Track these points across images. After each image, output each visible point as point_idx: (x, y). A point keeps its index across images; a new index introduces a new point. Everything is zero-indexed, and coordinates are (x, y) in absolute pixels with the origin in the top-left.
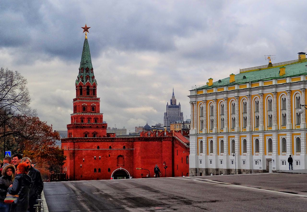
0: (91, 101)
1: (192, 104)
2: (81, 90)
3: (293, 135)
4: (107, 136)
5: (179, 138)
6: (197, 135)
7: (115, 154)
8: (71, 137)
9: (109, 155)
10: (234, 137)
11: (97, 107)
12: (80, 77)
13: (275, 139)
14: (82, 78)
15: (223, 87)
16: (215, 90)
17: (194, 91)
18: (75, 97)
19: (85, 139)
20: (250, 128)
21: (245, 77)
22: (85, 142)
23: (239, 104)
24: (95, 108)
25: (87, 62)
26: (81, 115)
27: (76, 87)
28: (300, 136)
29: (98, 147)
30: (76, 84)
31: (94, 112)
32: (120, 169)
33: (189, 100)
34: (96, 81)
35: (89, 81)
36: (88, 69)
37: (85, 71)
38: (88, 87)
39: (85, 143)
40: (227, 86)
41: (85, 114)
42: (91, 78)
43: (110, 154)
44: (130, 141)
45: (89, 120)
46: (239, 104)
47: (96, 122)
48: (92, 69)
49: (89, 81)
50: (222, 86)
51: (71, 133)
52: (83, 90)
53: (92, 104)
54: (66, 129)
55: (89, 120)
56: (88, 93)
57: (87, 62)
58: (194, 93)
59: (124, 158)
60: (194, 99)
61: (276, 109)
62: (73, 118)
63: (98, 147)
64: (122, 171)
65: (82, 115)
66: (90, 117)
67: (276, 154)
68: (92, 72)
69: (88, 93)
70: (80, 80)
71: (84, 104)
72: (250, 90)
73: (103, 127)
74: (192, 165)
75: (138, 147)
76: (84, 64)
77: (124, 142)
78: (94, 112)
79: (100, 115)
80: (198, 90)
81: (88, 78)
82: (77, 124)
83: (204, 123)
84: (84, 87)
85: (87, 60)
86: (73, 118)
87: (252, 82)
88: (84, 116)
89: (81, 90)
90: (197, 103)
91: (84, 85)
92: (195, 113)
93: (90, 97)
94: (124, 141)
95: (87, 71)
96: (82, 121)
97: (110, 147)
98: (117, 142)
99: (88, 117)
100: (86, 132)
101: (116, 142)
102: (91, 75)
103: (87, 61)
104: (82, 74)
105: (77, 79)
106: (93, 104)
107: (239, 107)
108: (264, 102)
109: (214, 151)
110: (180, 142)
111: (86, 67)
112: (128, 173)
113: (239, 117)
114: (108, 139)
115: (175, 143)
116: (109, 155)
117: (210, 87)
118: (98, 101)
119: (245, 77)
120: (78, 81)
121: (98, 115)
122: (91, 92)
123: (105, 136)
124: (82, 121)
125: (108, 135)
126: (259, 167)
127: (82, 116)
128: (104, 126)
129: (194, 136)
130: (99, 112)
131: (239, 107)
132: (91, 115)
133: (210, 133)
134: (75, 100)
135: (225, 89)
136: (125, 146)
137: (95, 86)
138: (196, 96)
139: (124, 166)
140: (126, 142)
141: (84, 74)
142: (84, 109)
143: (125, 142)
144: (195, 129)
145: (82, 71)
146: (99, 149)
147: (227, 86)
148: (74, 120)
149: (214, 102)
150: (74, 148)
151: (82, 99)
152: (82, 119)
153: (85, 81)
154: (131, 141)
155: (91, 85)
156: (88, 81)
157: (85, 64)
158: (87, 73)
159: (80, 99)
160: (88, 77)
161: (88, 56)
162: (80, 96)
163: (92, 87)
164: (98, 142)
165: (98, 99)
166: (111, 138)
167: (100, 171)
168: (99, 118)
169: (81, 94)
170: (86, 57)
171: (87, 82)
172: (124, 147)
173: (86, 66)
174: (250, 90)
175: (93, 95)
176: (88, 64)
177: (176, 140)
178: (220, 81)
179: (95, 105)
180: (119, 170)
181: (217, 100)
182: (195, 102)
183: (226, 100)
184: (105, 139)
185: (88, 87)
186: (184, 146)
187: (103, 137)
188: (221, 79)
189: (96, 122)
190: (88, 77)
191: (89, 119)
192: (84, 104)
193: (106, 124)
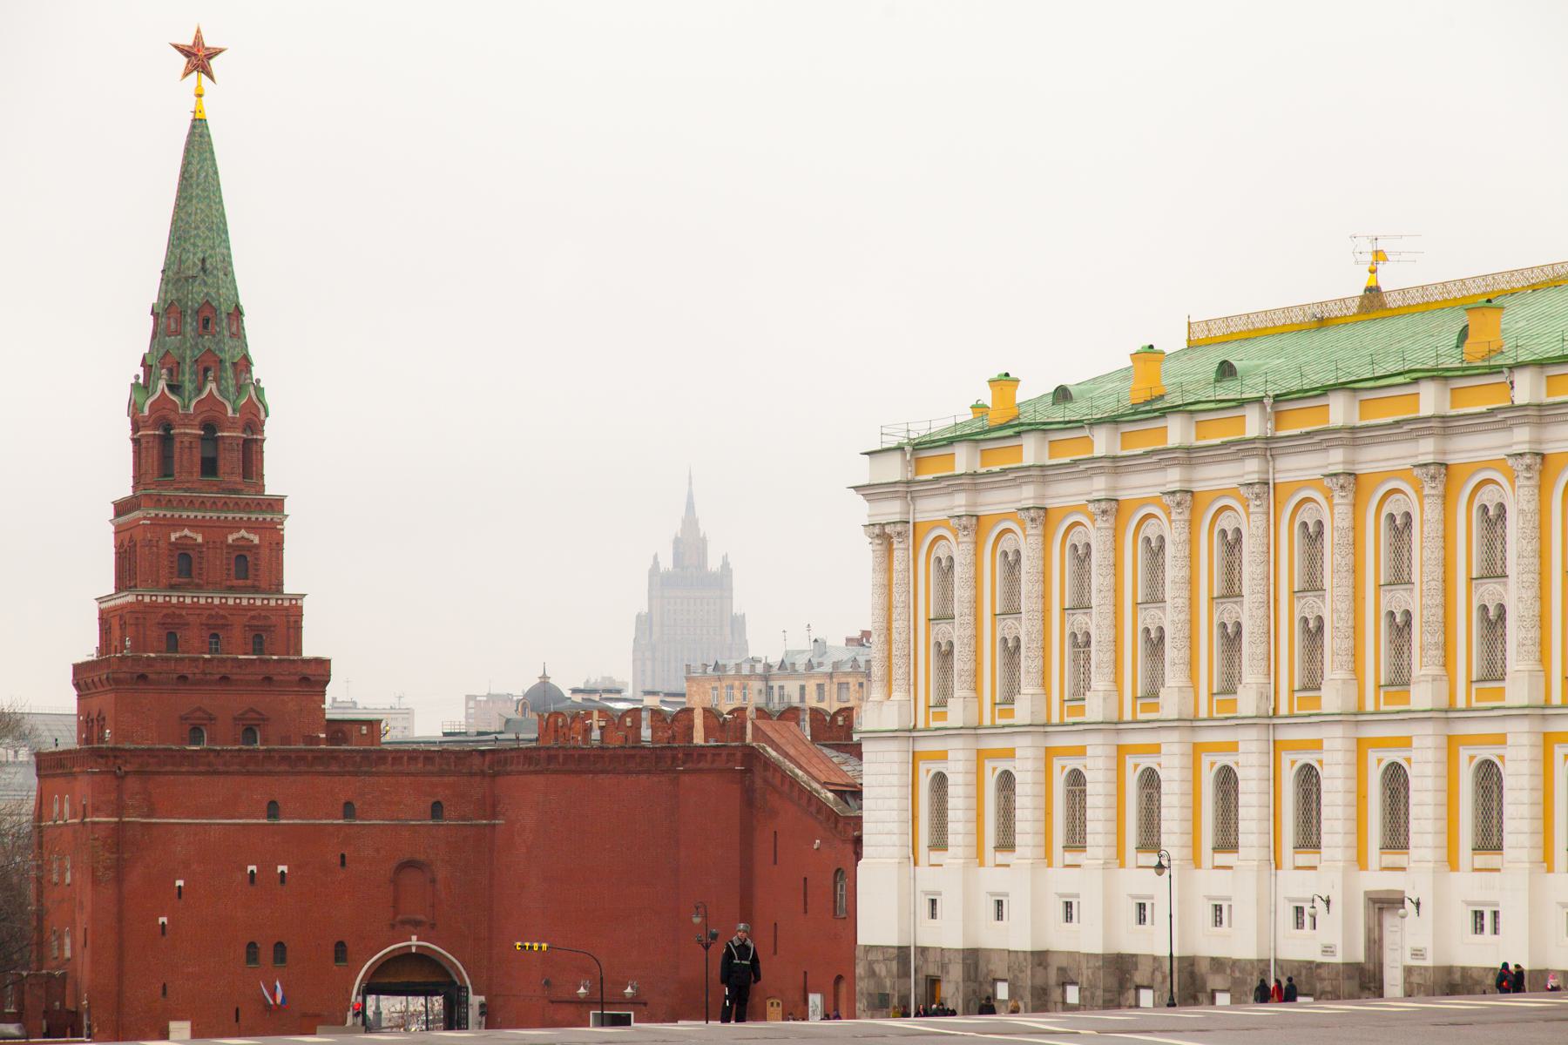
0: (230, 516)
1: (883, 536)
2: (166, 440)
3: (1362, 747)
4: (329, 740)
5: (786, 755)
6: (909, 733)
7: (377, 851)
8: (101, 739)
9: (343, 856)
10: (1080, 751)
11: (265, 553)
12: (162, 363)
13: (1339, 771)
14: (170, 371)
15: (1086, 432)
16: (1031, 451)
17: (898, 455)
18: (125, 490)
19: (186, 756)
20: (1262, 696)
21: (1226, 370)
22: (189, 773)
23: (1192, 542)
24: (257, 561)
25: (204, 269)
26: (167, 605)
27: (136, 427)
28: (1407, 754)
29: (273, 810)
30: (134, 410)
31: (249, 582)
33: (862, 512)
34: (259, 391)
35: (215, 393)
36: (214, 310)
37: (190, 326)
38: (210, 427)
39: (193, 778)
40: (1114, 421)
41: (188, 601)
42: (230, 373)
44: (472, 774)
45: (215, 636)
46: (1192, 542)
47: (261, 652)
48: (238, 313)
50: (1078, 424)
51: (101, 719)
52: (177, 446)
53: (235, 536)
54: (66, 700)
55: (215, 636)
56: (209, 467)
57: (204, 269)
58: (893, 469)
59: (433, 881)
60: (891, 510)
61: (1438, 573)
62: (115, 623)
63: (273, 810)
64: (422, 959)
65: (173, 606)
66: (224, 617)
68: (239, 335)
69: (209, 467)
70: (162, 384)
71: (186, 532)
72: (1268, 447)
73: (305, 680)
74: (880, 917)
75: (528, 805)
76: (186, 280)
77: (435, 779)
78: (249, 582)
79: (286, 603)
80: (919, 449)
81: (206, 370)
82: (136, 660)
83: (960, 662)
84: (185, 426)
85: (204, 252)
86: (108, 621)
87: (1278, 398)
89: (166, 440)
90: (911, 530)
91: (186, 416)
92: (898, 598)
93: (224, 491)
94: (432, 774)
95: (205, 326)
96: (172, 642)
97: (348, 810)
98: (392, 774)
100: (198, 714)
101: (386, 774)
102: (229, 355)
103: (203, 260)
104: (172, 341)
105: (137, 377)
106: (243, 533)
107: (1192, 558)
108: (1356, 528)
109: (951, 839)
110: (793, 782)
111: (200, 298)
112: (459, 974)
113: (1192, 622)
114: (332, 756)
115: (759, 783)
116: (343, 856)
117: (996, 430)
118: (276, 517)
119: (1226, 370)
120: (145, 387)
121: (273, 603)
122: (229, 461)
123: (318, 741)
124: (172, 642)
125: (340, 729)
126: (1331, 941)
127: (169, 611)
128: (317, 674)
129: (894, 746)
130: (280, 584)
131: (1192, 558)
132: (231, 602)
133: (994, 727)
134: (121, 508)
135: (1103, 443)
136: (445, 804)
137: (253, 420)
138: (907, 490)
139: (433, 926)
140: (451, 779)
141: (188, 346)
142: (186, 565)
143: (441, 774)
144: (898, 695)
145: (173, 326)
147: (1114, 421)
148: (116, 632)
149: (1029, 524)
151: (169, 503)
152: (171, 626)
153: (189, 387)
154: (483, 774)
155: (230, 413)
156: (211, 386)
157: (194, 277)
158: (201, 336)
159: (158, 502)
160: (208, 366)
161: (210, 229)
162: (159, 484)
163: (232, 424)
164: (270, 773)
165: (276, 504)
166: (358, 749)
167: (283, 960)
169: (166, 468)
170: (197, 236)
171: (204, 396)
172: (437, 810)
173: (197, 294)
174: (1268, 447)
175: (239, 479)
176: (210, 281)
177: (768, 764)
178: (1062, 395)
179: (256, 541)
180: (404, 957)
181: (1043, 516)
182: (899, 528)
183: (1104, 512)
184: (319, 757)
185: (210, 427)
186: (821, 805)
187: (303, 747)
188: (1069, 382)
189: (258, 645)
190: (208, 366)
191: (216, 626)
192: (186, 532)
193: (323, 665)
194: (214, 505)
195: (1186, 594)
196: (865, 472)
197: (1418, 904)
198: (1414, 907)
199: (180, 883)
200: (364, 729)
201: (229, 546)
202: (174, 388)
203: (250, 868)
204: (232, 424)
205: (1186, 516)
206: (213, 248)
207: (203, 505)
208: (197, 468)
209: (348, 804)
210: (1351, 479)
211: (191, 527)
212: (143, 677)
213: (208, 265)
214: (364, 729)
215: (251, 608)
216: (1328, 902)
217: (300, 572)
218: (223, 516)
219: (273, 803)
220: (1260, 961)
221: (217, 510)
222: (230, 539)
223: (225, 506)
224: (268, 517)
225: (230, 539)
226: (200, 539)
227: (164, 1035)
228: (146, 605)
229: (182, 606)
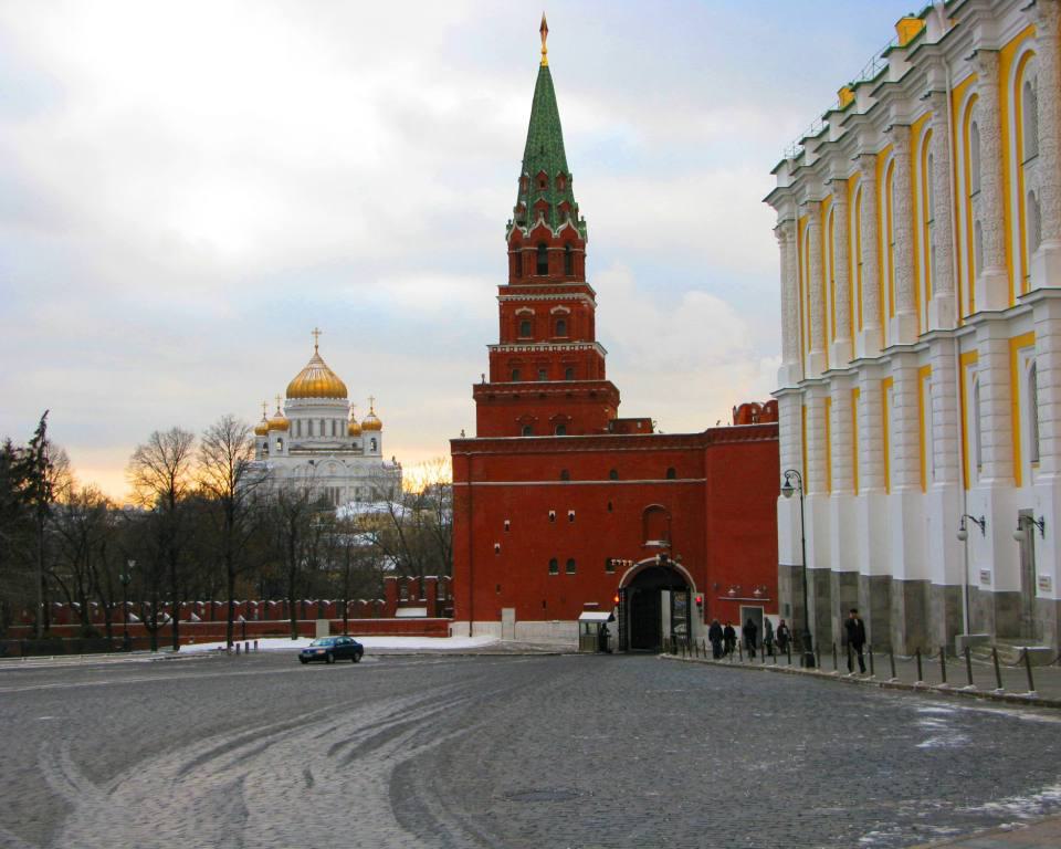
4: (611, 432)
25: (542, 153)
32: (654, 562)
34: (583, 223)
35: (544, 223)
42: (555, 211)
43: (612, 501)
49: (544, 223)
67: (997, 477)
71: (525, 309)
88: (522, 357)
95: (543, 185)
99: (538, 359)
103: (542, 148)
105: (510, 221)
106: (560, 307)
116: (610, 505)
146: (567, 482)
150: (470, 486)
153: (529, 221)
168: (595, 363)
179: (569, 311)
191: (542, 362)
192: (525, 309)
194: (542, 291)
195: (908, 224)
196: (772, 183)
197: (1042, 524)
198: (978, 527)
199: (507, 522)
200: (639, 425)
201: (552, 316)
202: (521, 223)
203: (552, 512)
204: (556, 243)
205: (905, 149)
206: (547, 139)
207: (535, 291)
208: (535, 269)
209: (613, 471)
210: (993, 55)
211: (529, 306)
212: (492, 397)
213: (545, 150)
214: (639, 425)
215: (564, 352)
216: (983, 523)
217: (607, 329)
218: (547, 297)
219: (564, 471)
220: (948, 587)
221: (545, 294)
222: (552, 312)
223: (549, 291)
224: (576, 295)
225: (552, 312)
226: (533, 312)
227: (498, 618)
228: (498, 354)
229: (521, 353)
